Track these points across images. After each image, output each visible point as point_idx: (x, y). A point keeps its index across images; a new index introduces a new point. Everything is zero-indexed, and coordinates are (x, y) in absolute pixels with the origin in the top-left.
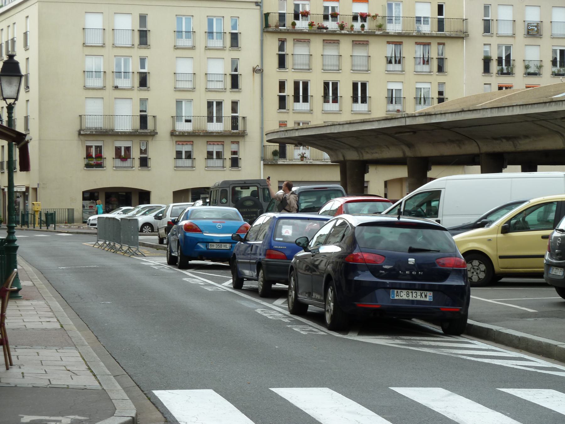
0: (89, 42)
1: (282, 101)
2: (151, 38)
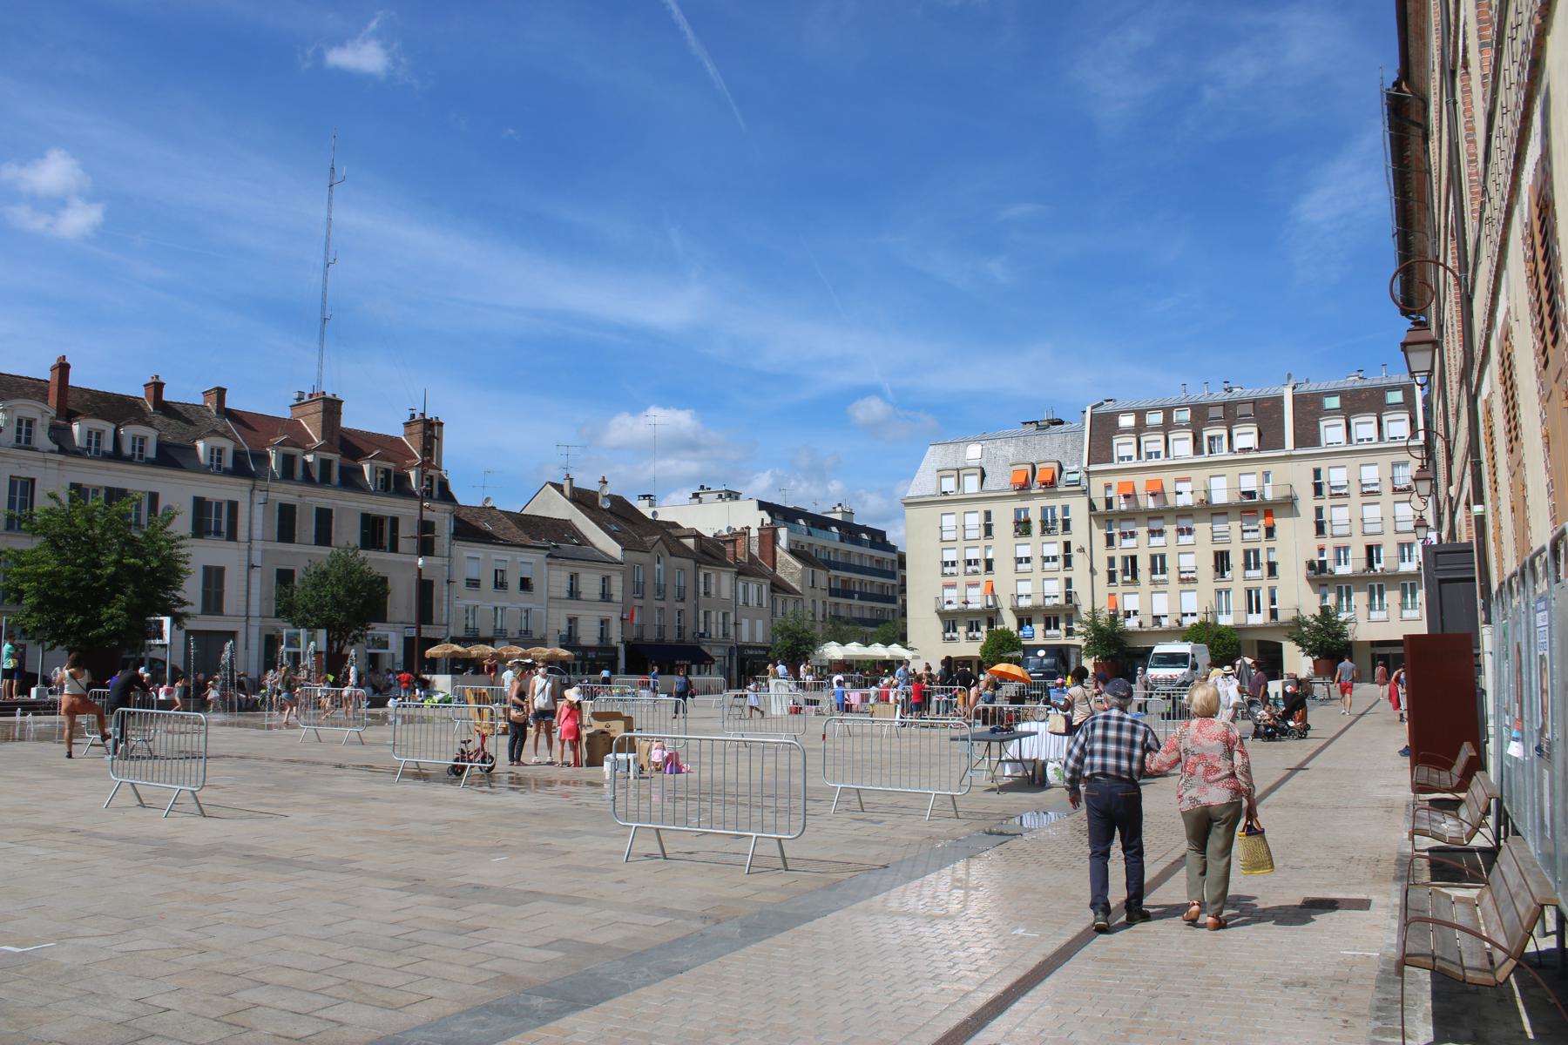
0: (946, 536)
1: (1112, 577)
2: (994, 530)
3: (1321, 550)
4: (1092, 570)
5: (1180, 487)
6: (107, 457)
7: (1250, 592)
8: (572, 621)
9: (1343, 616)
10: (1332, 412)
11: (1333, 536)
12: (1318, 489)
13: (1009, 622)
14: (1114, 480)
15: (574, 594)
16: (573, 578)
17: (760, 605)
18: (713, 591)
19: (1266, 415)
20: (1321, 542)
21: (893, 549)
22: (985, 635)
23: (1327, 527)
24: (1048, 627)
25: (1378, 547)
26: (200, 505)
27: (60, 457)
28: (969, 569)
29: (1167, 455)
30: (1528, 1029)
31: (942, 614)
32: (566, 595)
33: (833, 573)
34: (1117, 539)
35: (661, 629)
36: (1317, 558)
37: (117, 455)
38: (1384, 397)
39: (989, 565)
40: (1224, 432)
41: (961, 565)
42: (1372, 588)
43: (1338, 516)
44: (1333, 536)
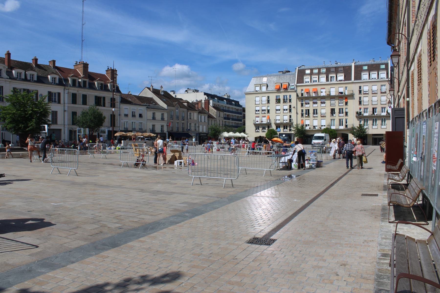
0: (257, 103)
1: (302, 115)
2: (270, 101)
3: (360, 109)
4: (297, 113)
5: (322, 90)
6: (23, 80)
7: (340, 120)
8: (153, 126)
9: (365, 127)
10: (365, 71)
11: (364, 105)
12: (360, 92)
13: (274, 127)
14: (304, 88)
15: (154, 118)
16: (154, 114)
17: (205, 122)
18: (192, 118)
19: (347, 71)
20: (360, 106)
21: (241, 106)
22: (267, 131)
23: (362, 102)
24: (284, 129)
25: (376, 108)
26: (50, 93)
27: (10, 80)
28: (263, 112)
29: (319, 81)
30: (415, 218)
31: (255, 125)
32: (152, 119)
33: (225, 113)
34: (304, 104)
35: (178, 128)
36: (359, 111)
37: (26, 80)
38: (380, 67)
39: (268, 111)
40: (335, 75)
41: (261, 111)
42: (373, 119)
43: (365, 99)
44: (364, 105)
